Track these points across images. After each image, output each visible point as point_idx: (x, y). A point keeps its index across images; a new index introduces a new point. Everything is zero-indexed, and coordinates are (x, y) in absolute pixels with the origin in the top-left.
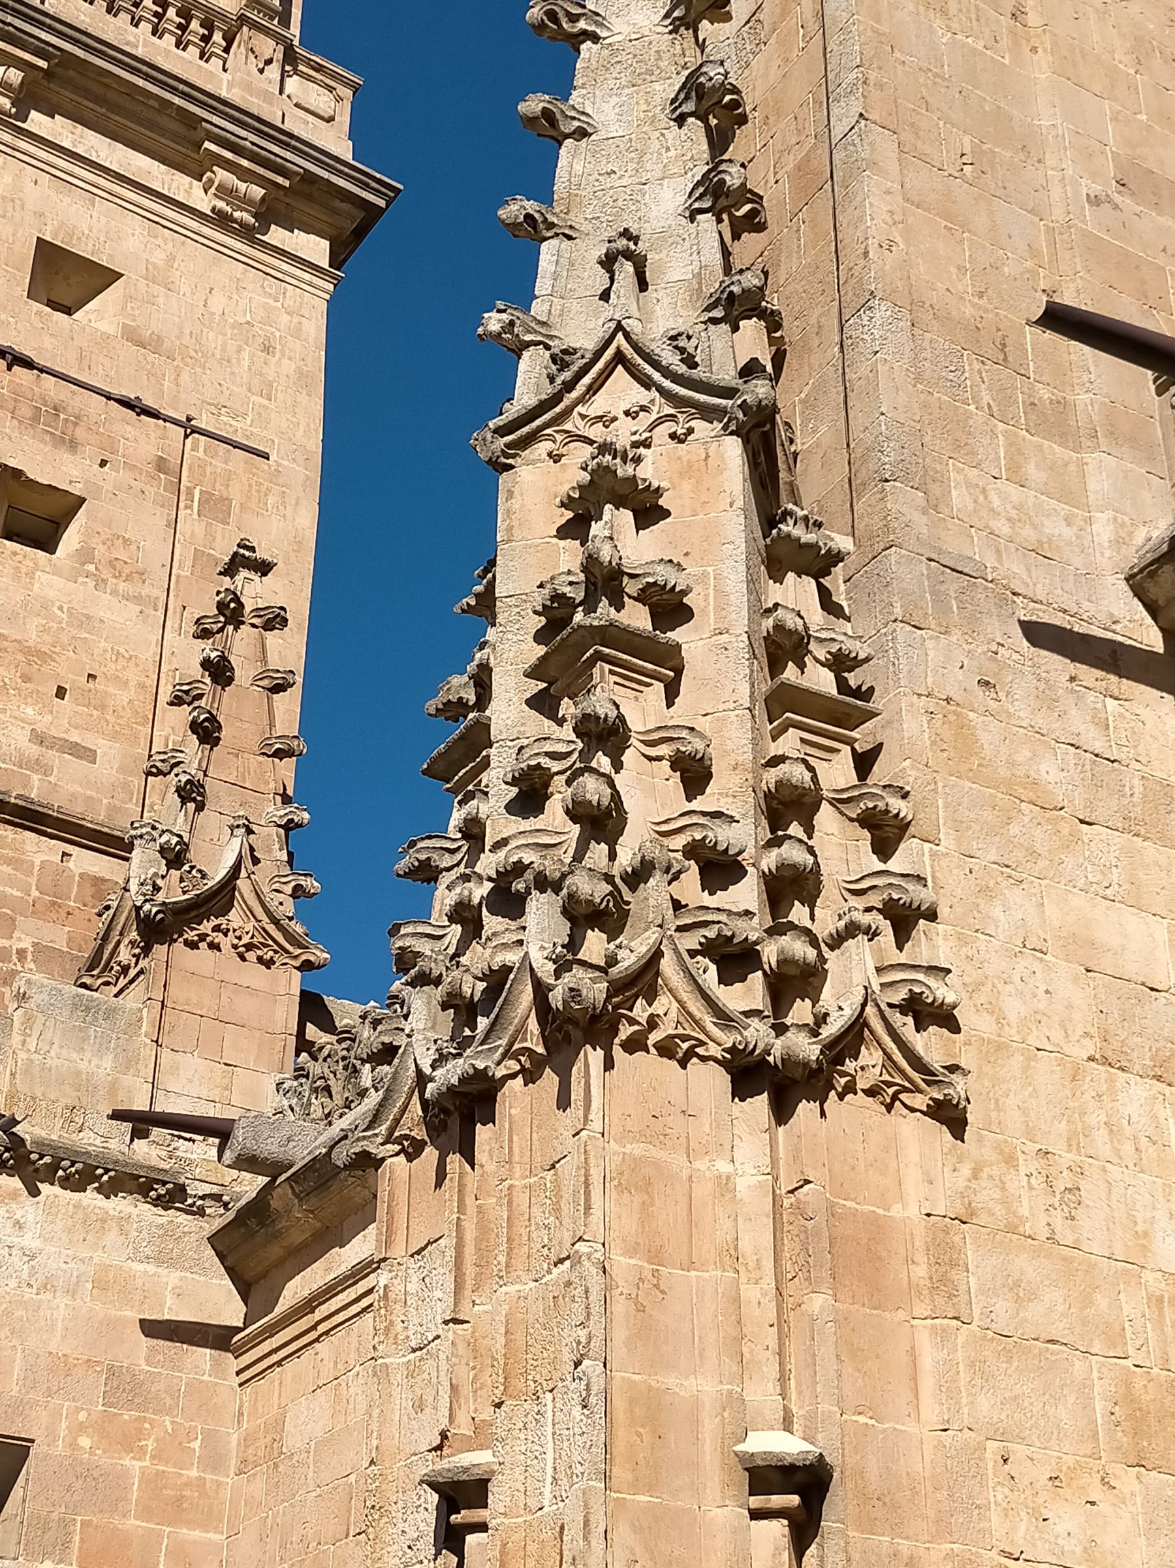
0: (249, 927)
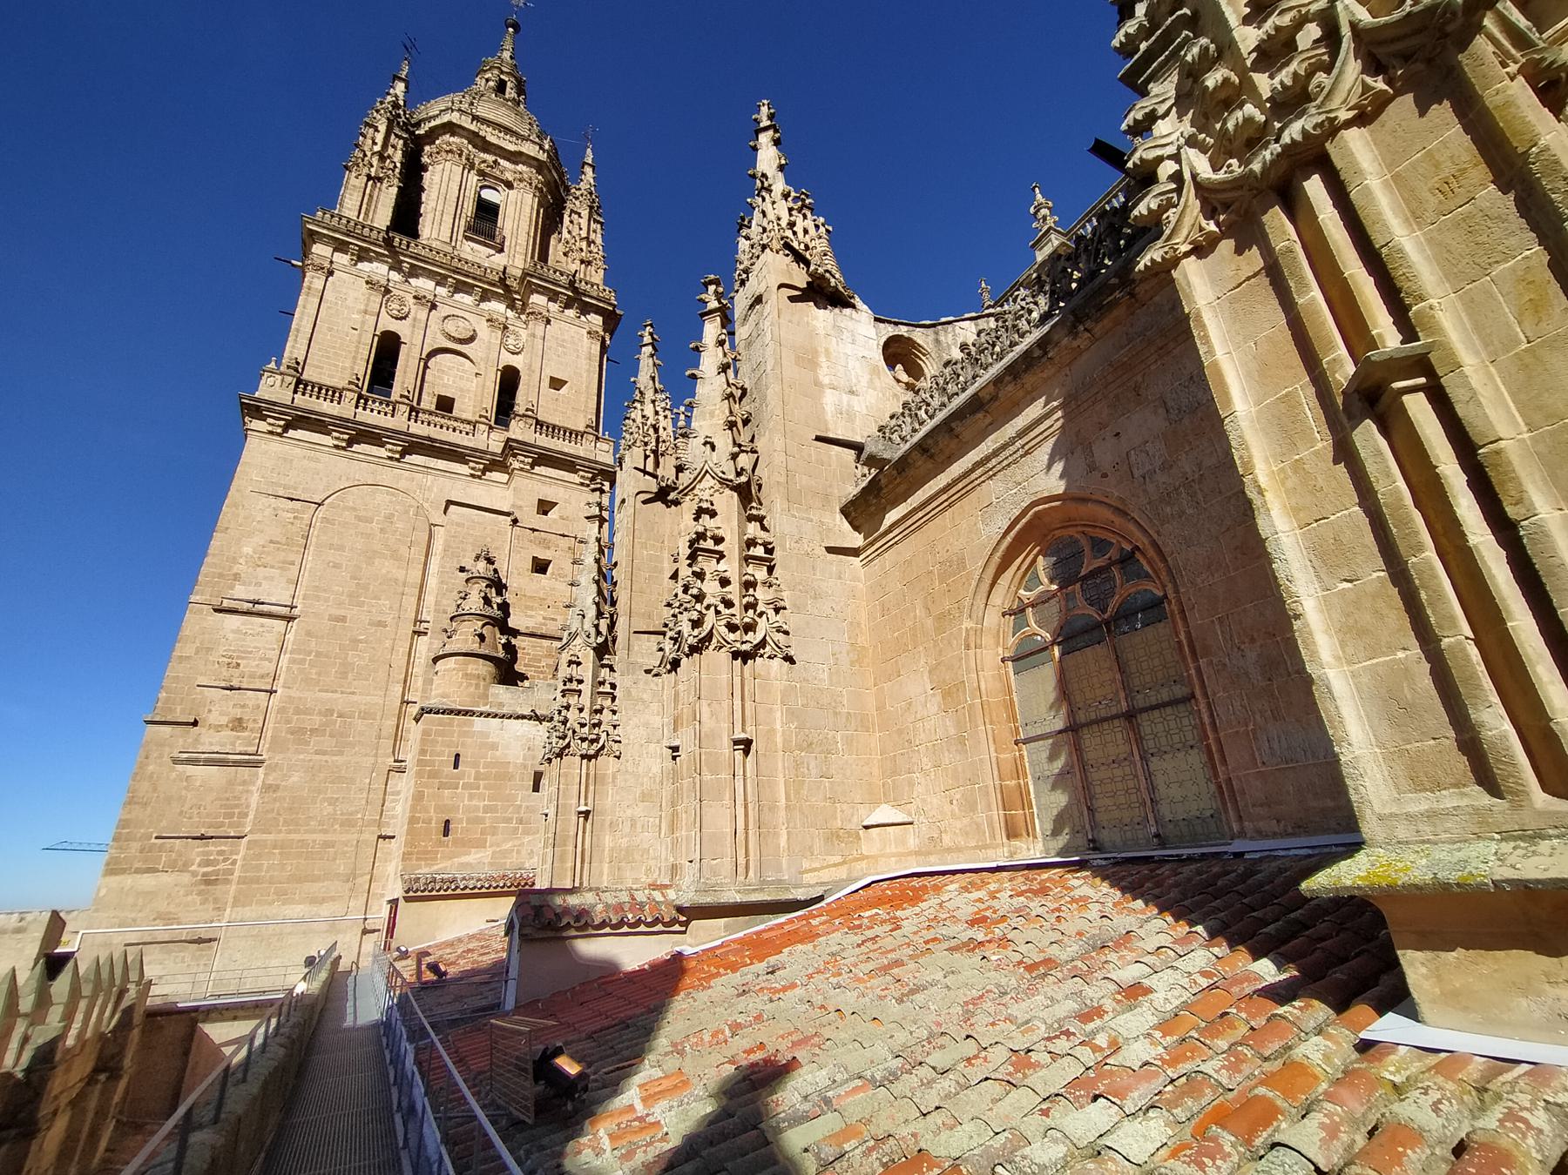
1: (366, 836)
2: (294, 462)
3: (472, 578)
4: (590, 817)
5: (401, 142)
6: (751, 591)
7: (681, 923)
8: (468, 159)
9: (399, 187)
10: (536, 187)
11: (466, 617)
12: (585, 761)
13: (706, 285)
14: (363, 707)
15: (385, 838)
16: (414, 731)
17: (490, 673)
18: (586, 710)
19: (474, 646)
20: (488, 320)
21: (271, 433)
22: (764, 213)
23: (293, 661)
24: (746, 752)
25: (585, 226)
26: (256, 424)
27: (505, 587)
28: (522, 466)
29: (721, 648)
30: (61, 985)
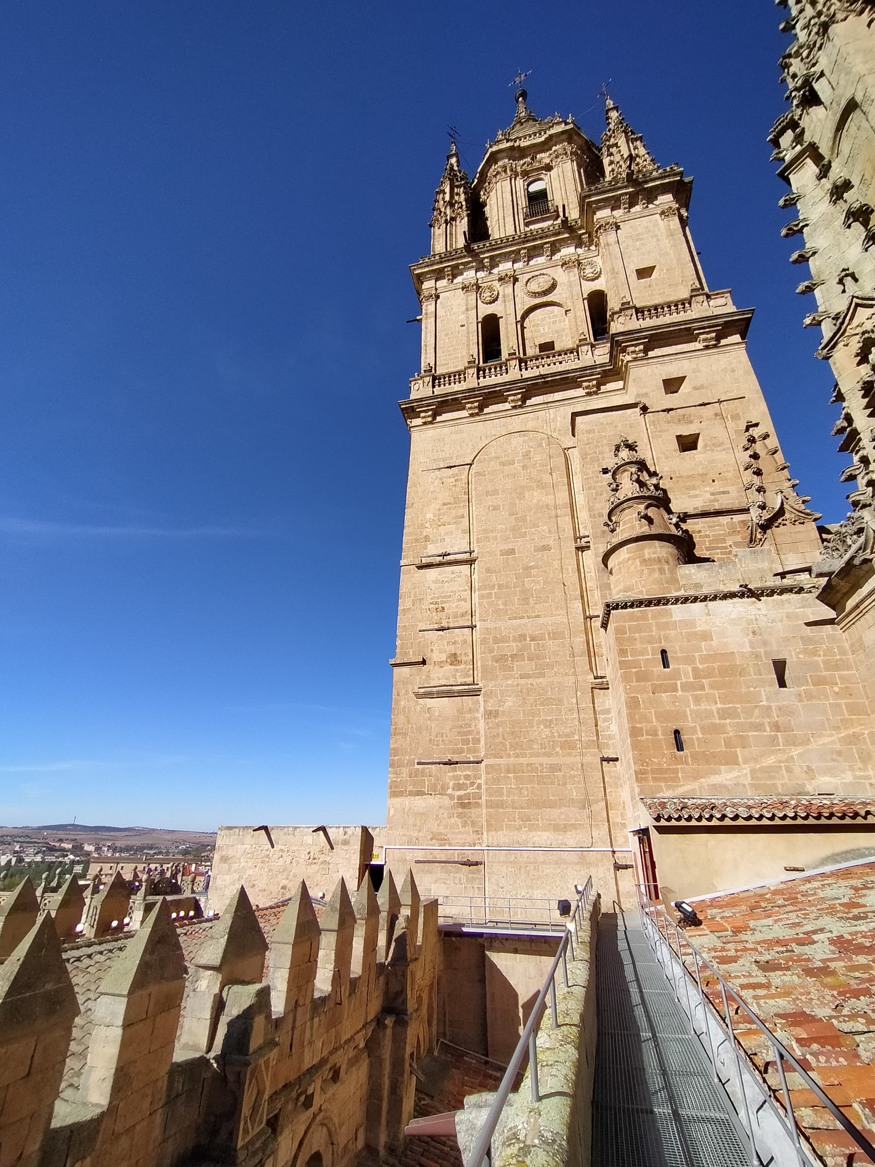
0: (793, 516)
1: (588, 759)
2: (446, 439)
14: (550, 628)
15: (609, 760)
20: (562, 266)
21: (425, 423)
23: (481, 597)
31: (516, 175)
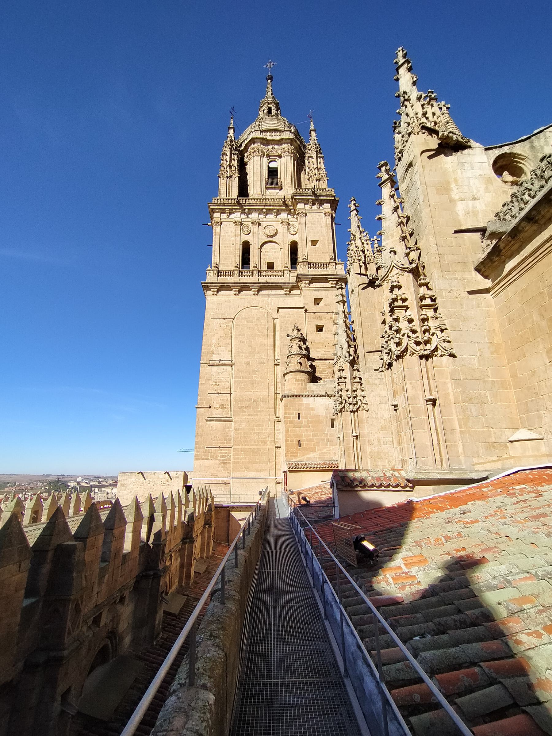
3: (293, 339)
4: (358, 438)
5: (236, 156)
6: (426, 323)
7: (410, 487)
8: (262, 152)
9: (238, 177)
10: (291, 152)
11: (293, 356)
12: (352, 414)
13: (380, 168)
16: (281, 405)
17: (306, 378)
18: (350, 391)
19: (298, 368)
20: (281, 223)
22: (407, 115)
23: (235, 381)
24: (434, 405)
25: (315, 163)
26: (209, 293)
27: (306, 340)
28: (305, 285)
29: (413, 354)
30: (191, 495)
31: (264, 155)
